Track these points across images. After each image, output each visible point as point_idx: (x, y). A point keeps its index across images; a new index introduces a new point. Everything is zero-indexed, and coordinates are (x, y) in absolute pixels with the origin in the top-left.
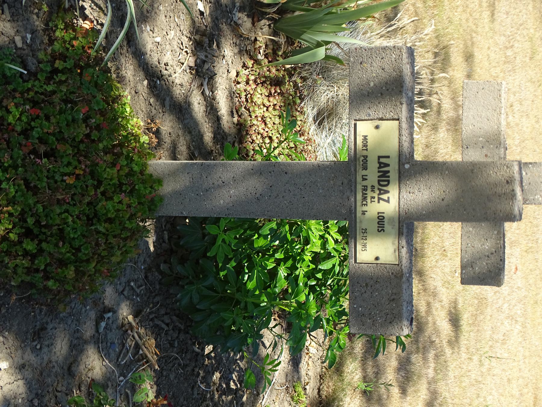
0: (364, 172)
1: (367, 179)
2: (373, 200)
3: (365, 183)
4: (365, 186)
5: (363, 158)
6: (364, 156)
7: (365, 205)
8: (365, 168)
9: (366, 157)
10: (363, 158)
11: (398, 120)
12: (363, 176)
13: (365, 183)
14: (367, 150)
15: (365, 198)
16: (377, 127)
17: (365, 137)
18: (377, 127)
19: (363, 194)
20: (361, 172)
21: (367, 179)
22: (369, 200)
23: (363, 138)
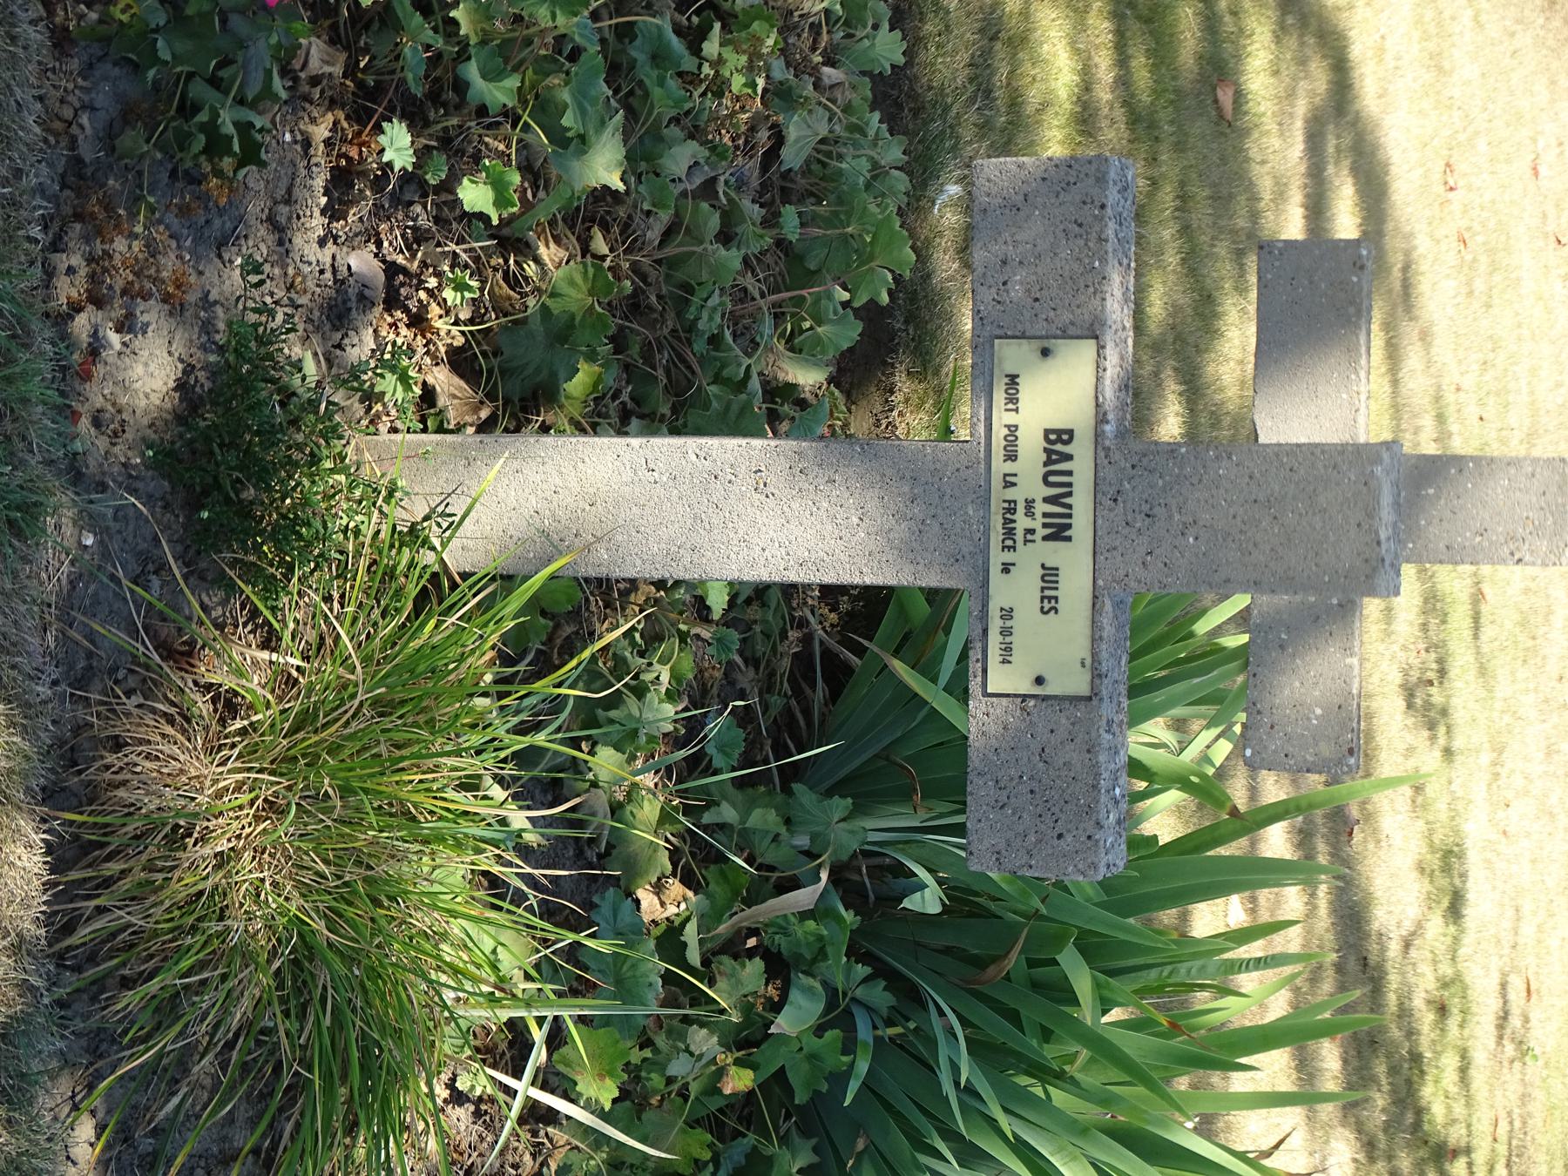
0: (1009, 467)
2: (1029, 537)
3: (1011, 494)
4: (1009, 502)
5: (1006, 431)
6: (1008, 427)
7: (1009, 548)
8: (1011, 456)
9: (1013, 429)
10: (1006, 431)
11: (1097, 338)
13: (1011, 494)
14: (1017, 410)
15: (1010, 533)
19: (1007, 521)
21: (1014, 484)
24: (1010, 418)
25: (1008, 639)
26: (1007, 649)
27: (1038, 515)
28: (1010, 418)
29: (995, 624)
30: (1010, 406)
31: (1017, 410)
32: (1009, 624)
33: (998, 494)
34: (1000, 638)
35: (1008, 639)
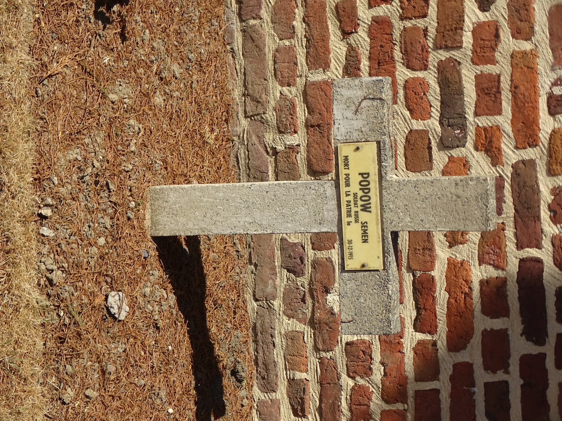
0: (347, 189)
1: (349, 195)
3: (348, 198)
5: (345, 176)
8: (348, 185)
9: (347, 175)
10: (345, 176)
12: (346, 192)
13: (348, 198)
14: (348, 169)
16: (358, 149)
17: (346, 158)
18: (358, 149)
20: (343, 189)
21: (349, 195)
22: (353, 213)
23: (344, 158)
24: (347, 171)
25: (351, 251)
26: (351, 254)
27: (359, 205)
28: (347, 171)
29: (346, 245)
30: (346, 167)
31: (348, 169)
32: (351, 245)
33: (344, 199)
34: (348, 251)
35: (351, 251)
